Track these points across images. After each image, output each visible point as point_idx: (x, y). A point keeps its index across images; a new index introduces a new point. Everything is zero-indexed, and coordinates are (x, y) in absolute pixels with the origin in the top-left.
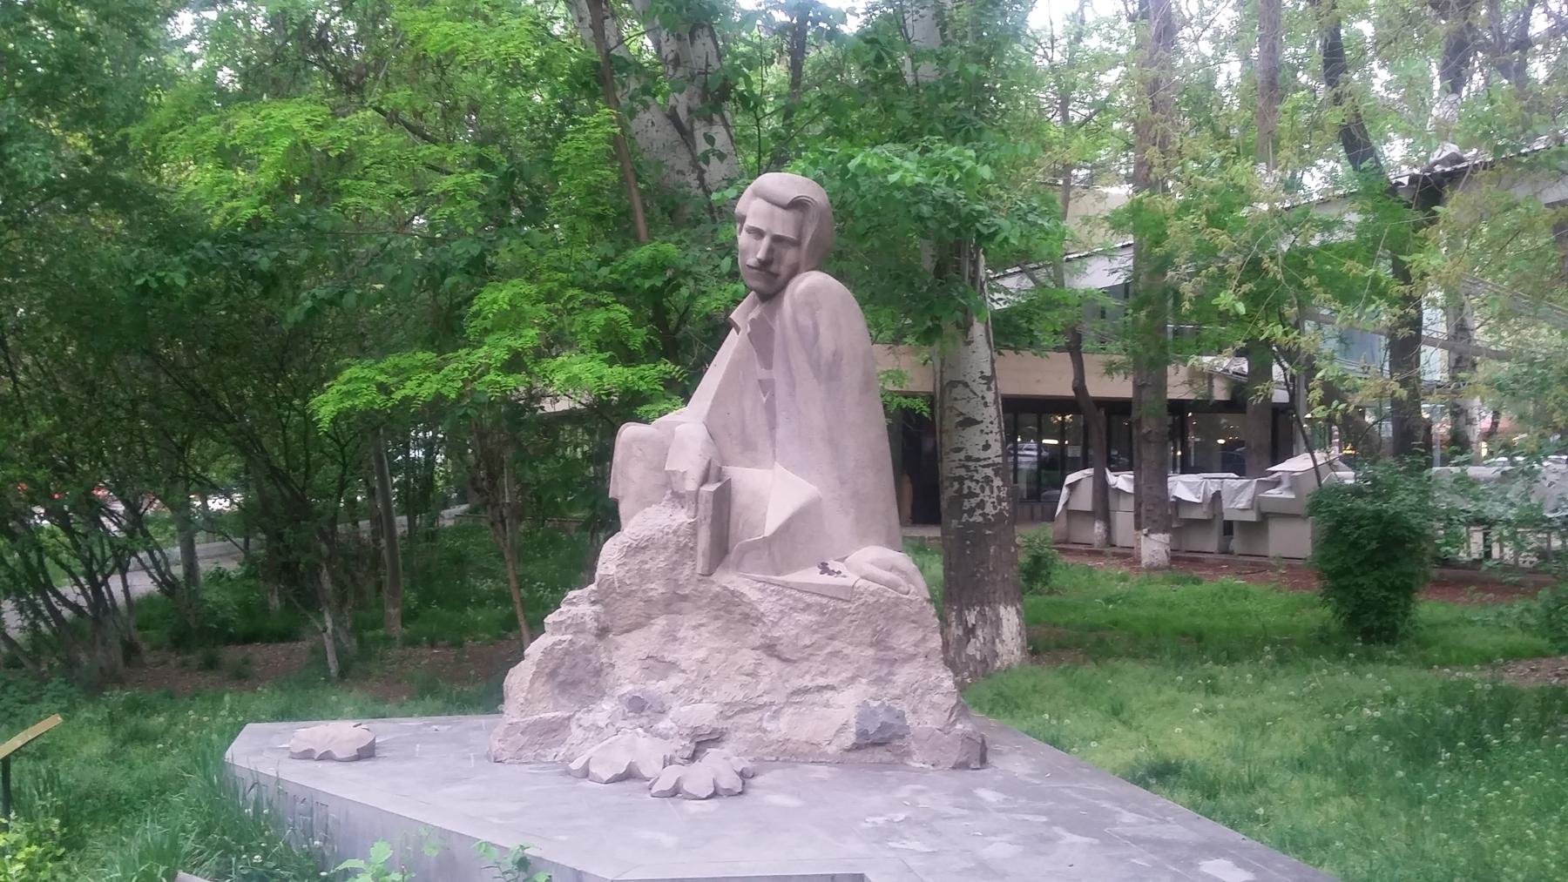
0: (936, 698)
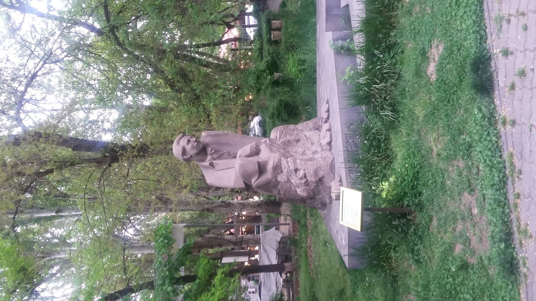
0: (305, 124)
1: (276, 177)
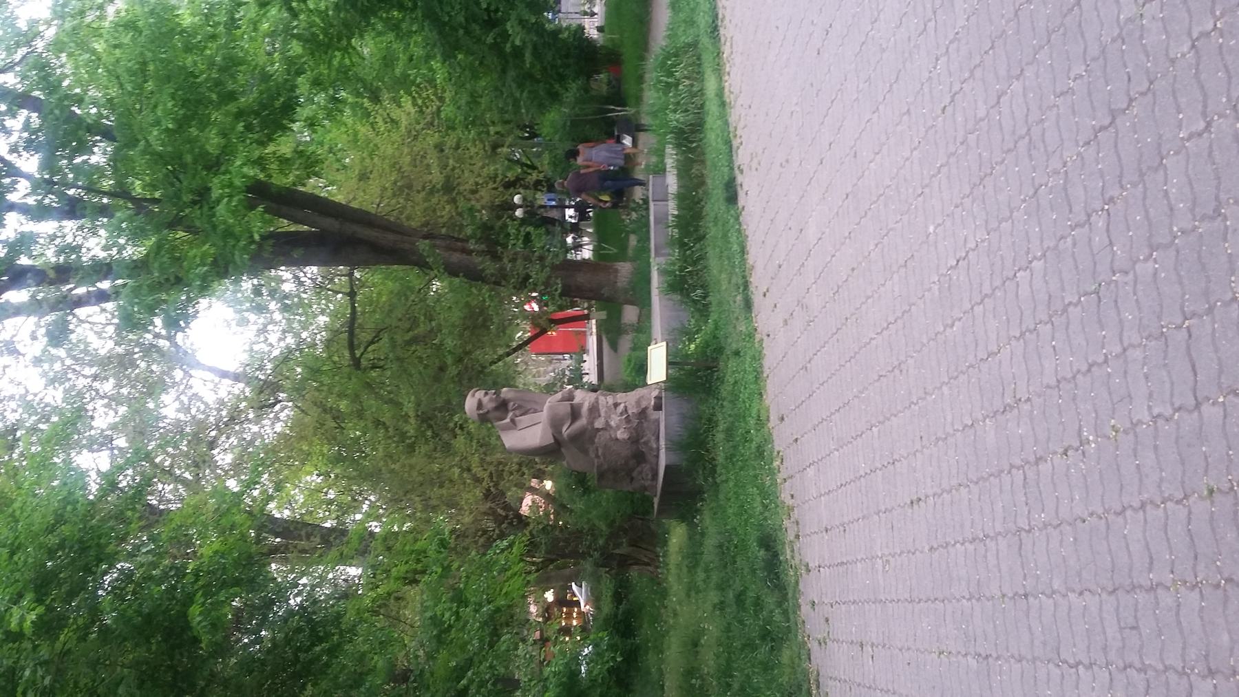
1: (592, 423)
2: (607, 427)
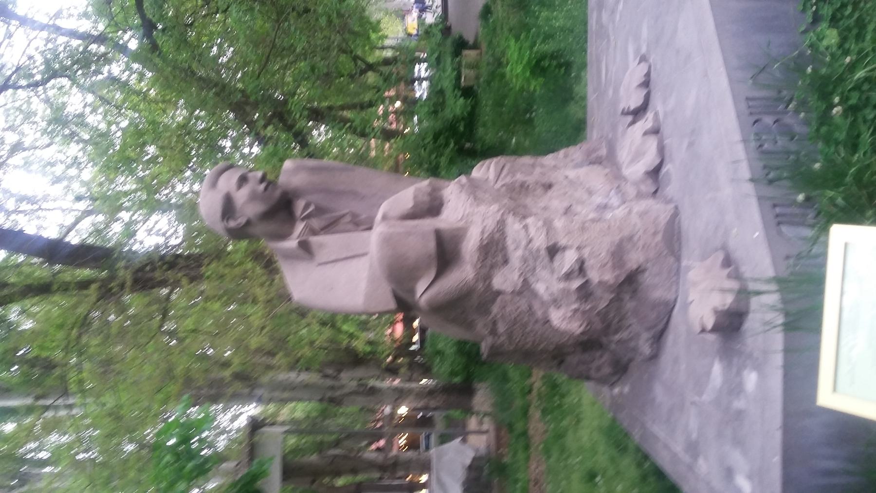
1: (487, 278)
2: (525, 288)
